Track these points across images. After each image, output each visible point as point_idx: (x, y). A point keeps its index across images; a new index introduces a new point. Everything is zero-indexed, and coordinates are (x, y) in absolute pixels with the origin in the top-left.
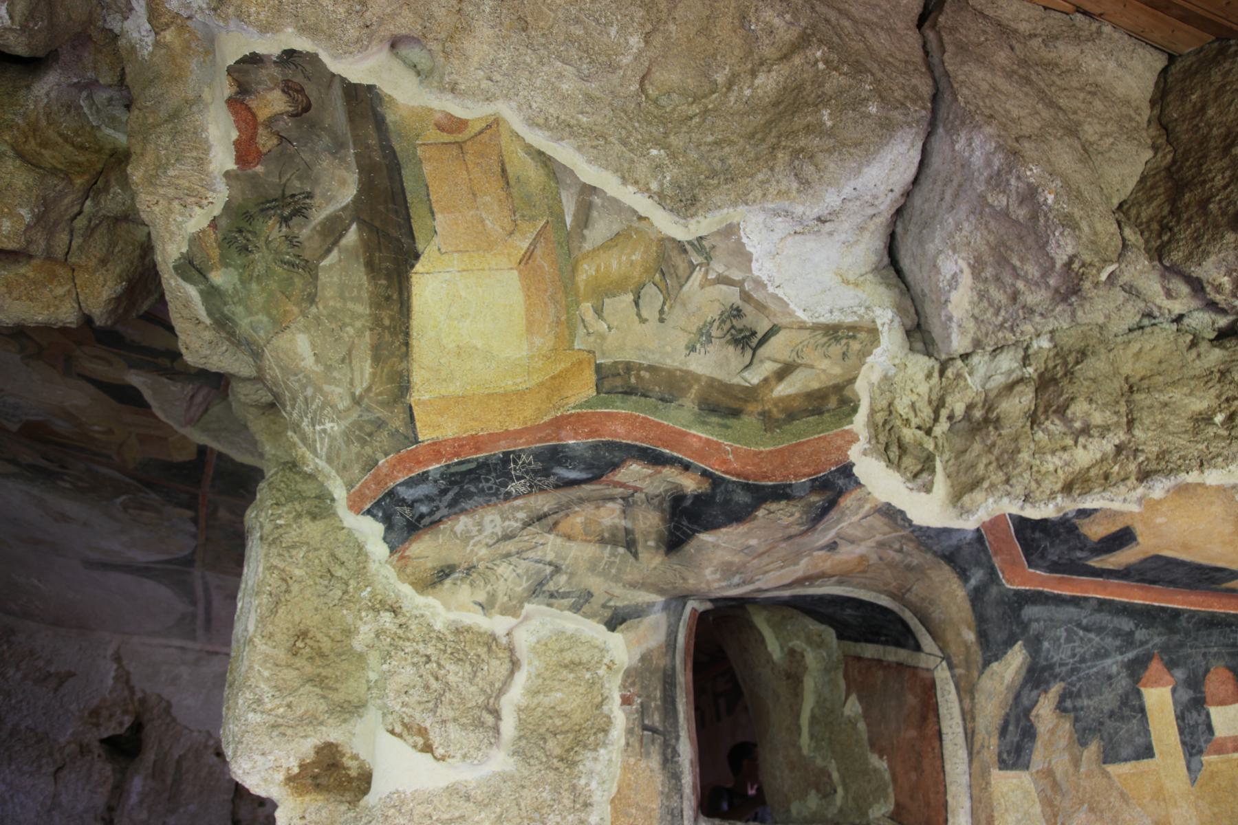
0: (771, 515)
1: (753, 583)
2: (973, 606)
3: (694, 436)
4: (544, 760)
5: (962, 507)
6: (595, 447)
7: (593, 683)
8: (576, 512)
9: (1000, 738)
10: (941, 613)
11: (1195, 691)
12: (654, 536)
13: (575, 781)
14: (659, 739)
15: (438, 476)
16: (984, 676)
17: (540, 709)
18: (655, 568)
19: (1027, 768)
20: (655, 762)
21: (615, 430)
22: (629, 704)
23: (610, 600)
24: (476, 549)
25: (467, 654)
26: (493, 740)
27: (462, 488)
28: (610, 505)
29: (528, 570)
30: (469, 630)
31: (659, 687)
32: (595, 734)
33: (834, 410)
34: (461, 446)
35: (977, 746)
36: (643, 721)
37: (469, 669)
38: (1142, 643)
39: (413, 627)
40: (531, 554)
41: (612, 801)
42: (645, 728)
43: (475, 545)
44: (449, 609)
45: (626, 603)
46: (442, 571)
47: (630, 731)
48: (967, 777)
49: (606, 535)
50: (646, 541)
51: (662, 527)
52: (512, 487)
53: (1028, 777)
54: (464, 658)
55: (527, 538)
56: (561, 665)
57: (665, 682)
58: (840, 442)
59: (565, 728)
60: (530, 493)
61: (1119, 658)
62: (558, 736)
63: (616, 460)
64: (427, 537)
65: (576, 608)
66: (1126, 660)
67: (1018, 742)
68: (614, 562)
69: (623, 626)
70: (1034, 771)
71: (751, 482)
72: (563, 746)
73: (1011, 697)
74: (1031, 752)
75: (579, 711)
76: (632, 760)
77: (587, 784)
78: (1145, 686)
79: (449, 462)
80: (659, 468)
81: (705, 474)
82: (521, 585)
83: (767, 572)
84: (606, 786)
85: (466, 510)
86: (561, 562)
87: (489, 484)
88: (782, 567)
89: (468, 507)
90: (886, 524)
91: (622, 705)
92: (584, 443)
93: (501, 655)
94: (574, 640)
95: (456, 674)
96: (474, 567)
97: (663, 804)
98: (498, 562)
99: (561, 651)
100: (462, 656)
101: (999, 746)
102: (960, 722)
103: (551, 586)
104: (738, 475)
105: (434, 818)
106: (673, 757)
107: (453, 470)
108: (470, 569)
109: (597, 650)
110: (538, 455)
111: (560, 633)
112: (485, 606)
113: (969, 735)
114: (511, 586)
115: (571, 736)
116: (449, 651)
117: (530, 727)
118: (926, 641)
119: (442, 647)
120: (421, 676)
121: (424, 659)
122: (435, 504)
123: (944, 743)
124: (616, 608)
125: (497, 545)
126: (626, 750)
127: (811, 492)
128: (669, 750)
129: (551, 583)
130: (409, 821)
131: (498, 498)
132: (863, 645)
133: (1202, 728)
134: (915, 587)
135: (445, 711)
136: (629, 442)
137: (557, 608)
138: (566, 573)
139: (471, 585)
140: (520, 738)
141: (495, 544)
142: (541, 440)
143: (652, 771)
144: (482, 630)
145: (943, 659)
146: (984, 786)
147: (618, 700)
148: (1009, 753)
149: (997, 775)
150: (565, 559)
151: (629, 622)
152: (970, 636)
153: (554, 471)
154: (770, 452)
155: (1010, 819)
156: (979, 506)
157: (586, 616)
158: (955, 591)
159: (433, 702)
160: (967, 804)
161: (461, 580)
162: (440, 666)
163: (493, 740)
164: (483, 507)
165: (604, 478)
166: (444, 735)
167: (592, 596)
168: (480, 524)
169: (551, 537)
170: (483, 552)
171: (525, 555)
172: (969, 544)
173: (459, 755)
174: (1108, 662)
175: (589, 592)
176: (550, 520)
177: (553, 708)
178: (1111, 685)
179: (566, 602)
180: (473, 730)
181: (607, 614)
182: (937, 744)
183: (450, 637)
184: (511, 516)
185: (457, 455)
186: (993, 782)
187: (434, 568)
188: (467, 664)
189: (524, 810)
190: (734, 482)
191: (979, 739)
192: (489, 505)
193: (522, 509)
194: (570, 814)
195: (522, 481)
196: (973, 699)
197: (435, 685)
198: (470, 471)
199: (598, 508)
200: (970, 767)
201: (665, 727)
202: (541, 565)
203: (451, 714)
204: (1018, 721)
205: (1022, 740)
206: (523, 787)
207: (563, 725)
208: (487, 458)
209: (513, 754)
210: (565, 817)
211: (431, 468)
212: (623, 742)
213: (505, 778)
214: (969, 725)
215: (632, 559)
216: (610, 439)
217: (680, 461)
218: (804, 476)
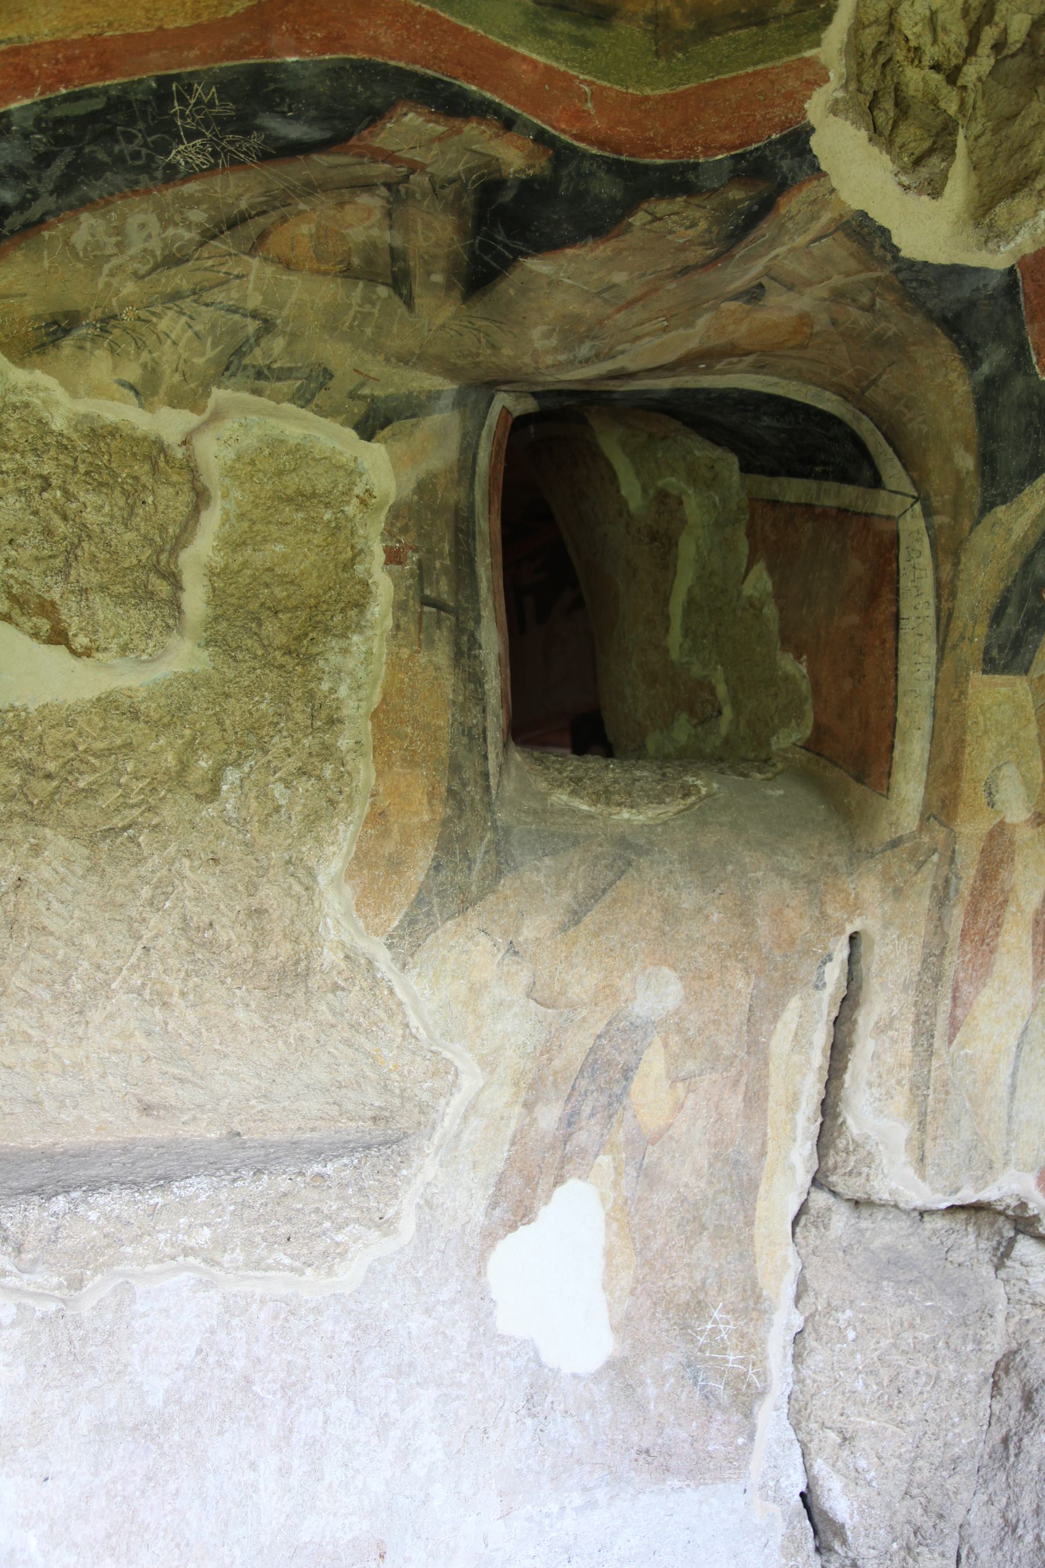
0: (657, 224)
1: (614, 357)
2: (979, 410)
3: (524, 58)
4: (260, 652)
5: (991, 226)
6: (337, 71)
7: (338, 528)
8: (300, 213)
9: (991, 626)
10: (924, 422)
12: (442, 264)
13: (313, 685)
14: (449, 620)
15: (29, 124)
16: (979, 527)
17: (248, 572)
18: (443, 326)
19: (1026, 672)
20: (442, 655)
21: (375, 38)
22: (399, 563)
23: (363, 385)
24: (115, 282)
25: (115, 475)
26: (171, 622)
27: (79, 152)
28: (364, 199)
29: (213, 326)
30: (114, 431)
31: (448, 536)
32: (343, 610)
33: (787, 16)
34: (70, 60)
35: (954, 636)
36: (422, 590)
37: (122, 502)
39: (11, 425)
40: (219, 296)
41: (374, 715)
42: (426, 601)
43: (112, 274)
44: (74, 394)
45: (391, 390)
46: (55, 323)
47: (400, 607)
48: (932, 683)
49: (356, 261)
50: (429, 273)
51: (457, 246)
52: (182, 154)
53: (1026, 685)
54: (111, 482)
55: (210, 263)
56: (280, 498)
57: (457, 530)
58: (792, 83)
59: (292, 602)
60: (213, 168)
62: (280, 616)
63: (378, 102)
64: (19, 256)
65: (303, 399)
67: (1018, 634)
68: (370, 314)
69: (387, 431)
70: (1036, 676)
71: (624, 158)
72: (290, 630)
73: (1018, 561)
74: (1036, 647)
75: (315, 574)
76: (405, 653)
77: (333, 690)
79: (48, 95)
80: (457, 123)
81: (542, 138)
82: (203, 354)
83: (638, 338)
84: (363, 693)
85: (91, 201)
86: (273, 312)
87: (134, 146)
88: (665, 330)
89: (94, 195)
90: (852, 254)
91: (386, 564)
92: (316, 63)
93: (175, 478)
94: (301, 455)
95: (99, 509)
96: (115, 317)
97: (455, 720)
98: (158, 309)
99: (280, 473)
100: (106, 477)
101: (988, 637)
102: (932, 601)
103: (257, 357)
104: (601, 144)
105: (81, 748)
106: (470, 649)
107: (59, 112)
108: (107, 321)
109: (341, 473)
110: (226, 85)
111: (275, 444)
112: (139, 388)
113: (943, 621)
114: (185, 355)
115: (303, 615)
116: (82, 468)
117: (234, 601)
118: (893, 472)
119: (70, 462)
120: (36, 513)
121: (38, 482)
122: (29, 185)
123: (901, 632)
124: (373, 398)
125: (154, 276)
126: (394, 637)
127: (730, 180)
128: (465, 638)
129: (257, 352)
130: (39, 754)
131: (153, 178)
132: (784, 480)
134: (884, 377)
135: (84, 574)
136: (402, 64)
137: (270, 398)
138: (284, 333)
139: (112, 351)
140: (216, 619)
141: (149, 273)
142: (230, 53)
143: (437, 669)
144: (138, 433)
145: (917, 499)
146: (955, 697)
147: (380, 556)
148: (1001, 649)
149: (977, 679)
150: (281, 307)
151: (396, 425)
152: (967, 462)
153: (258, 121)
154: (664, 98)
155: (988, 745)
156: (1021, 225)
157: (320, 412)
158: (951, 384)
159: (62, 557)
160: (927, 723)
161: (93, 340)
162: (67, 494)
163: (171, 622)
164: (124, 197)
165: (353, 141)
166: (87, 613)
167: (331, 377)
168: (119, 231)
169: (255, 262)
170: (129, 288)
171: (207, 297)
172: (991, 297)
173: (114, 646)
175: (325, 370)
176: (252, 229)
177: (270, 570)
179: (285, 386)
180: (136, 605)
181: (359, 409)
182: (890, 635)
183: (82, 444)
184: (177, 218)
185: (64, 79)
186: (970, 691)
187: (38, 317)
188: (117, 493)
189: (230, 731)
190: (594, 157)
191: (958, 625)
192: (135, 193)
193: (198, 203)
194: (306, 736)
195: (198, 142)
196: (956, 564)
197: (62, 528)
198: (93, 117)
199: (341, 205)
201: (457, 601)
202: (237, 317)
203: (95, 578)
204: (1023, 599)
205: (1025, 629)
206: (227, 696)
207: (289, 597)
208: (125, 88)
209: (207, 645)
210: (298, 741)
211: (13, 106)
212: (389, 623)
213: (194, 682)
214: (945, 605)
215: (402, 309)
216: (366, 56)
217: (495, 110)
218: (722, 148)
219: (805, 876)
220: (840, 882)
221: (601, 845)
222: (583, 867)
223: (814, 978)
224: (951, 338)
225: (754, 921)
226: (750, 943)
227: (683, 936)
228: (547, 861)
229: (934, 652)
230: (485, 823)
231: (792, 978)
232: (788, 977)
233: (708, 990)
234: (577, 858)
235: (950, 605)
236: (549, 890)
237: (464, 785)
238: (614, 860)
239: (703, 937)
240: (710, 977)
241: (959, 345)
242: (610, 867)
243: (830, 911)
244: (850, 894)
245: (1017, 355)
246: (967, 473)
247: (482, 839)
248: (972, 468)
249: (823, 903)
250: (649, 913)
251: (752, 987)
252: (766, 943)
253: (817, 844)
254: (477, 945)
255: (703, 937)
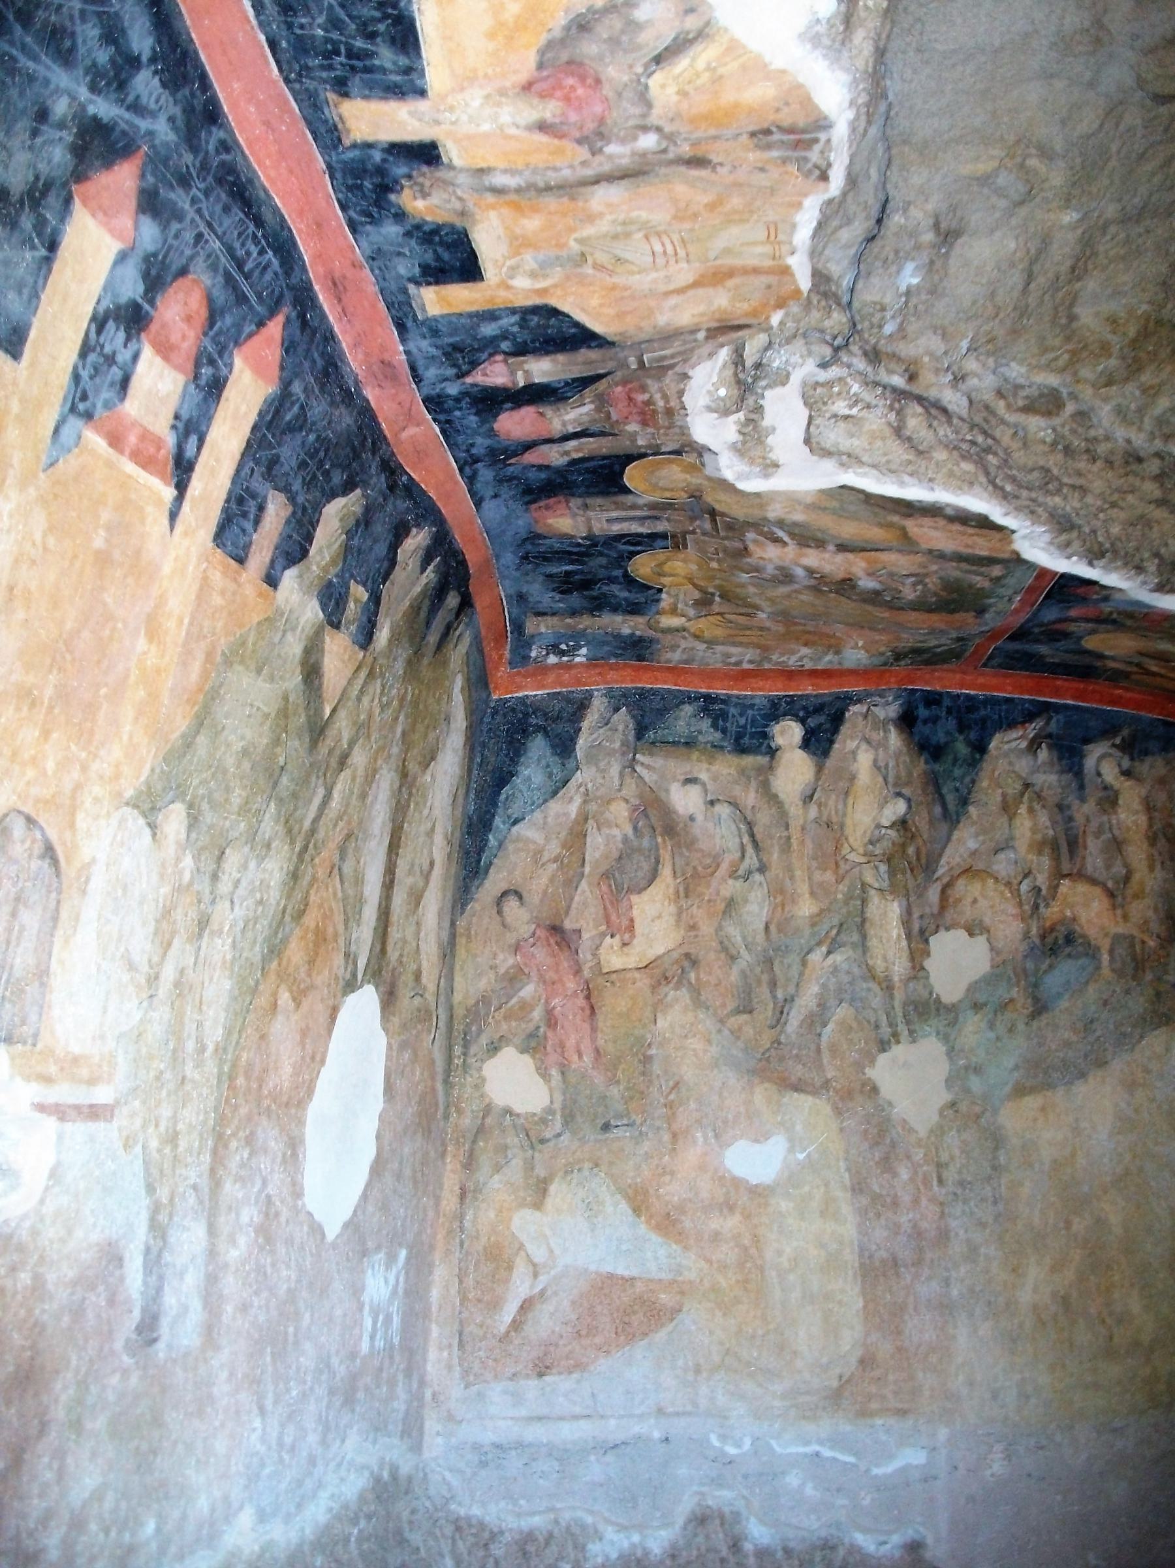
11: (146, 292)
38: (136, 107)
61: (83, 93)
66: (91, 110)
78: (85, 203)
133: (116, 373)
174: (61, 78)
178: (35, 133)
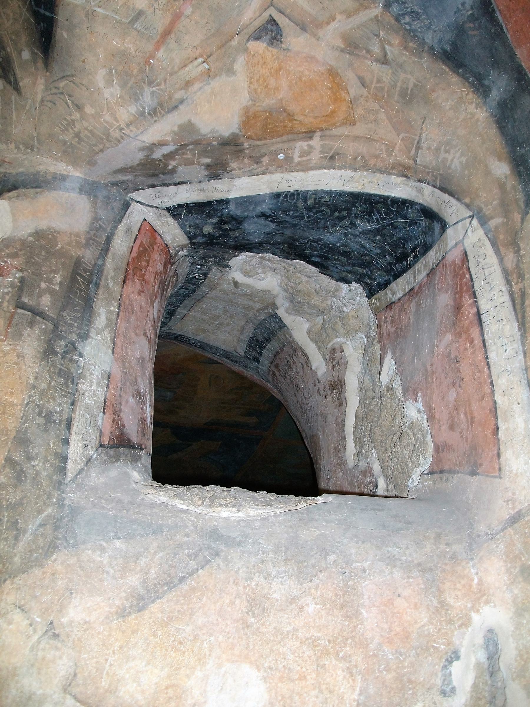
12: (24, 38)
36: (20, 297)
45: (21, 170)
48: (521, 357)
50: (20, 53)
69: (13, 193)
102: (504, 289)
113: (518, 301)
151: (21, 191)
182: (475, 332)
196: (517, 251)
200: (523, 344)
219: (419, 564)
220: (459, 568)
221: (187, 535)
222: (161, 554)
223: (439, 682)
224: (458, 74)
225: (358, 613)
226: (353, 638)
227: (270, 628)
228: (118, 543)
229: (516, 329)
230: (49, 497)
231: (410, 681)
232: (405, 679)
233: (300, 695)
234: (155, 544)
235: (521, 285)
236: (112, 571)
237: (29, 458)
238: (201, 550)
239: (296, 630)
240: (302, 678)
241: (467, 79)
242: (194, 556)
243: (450, 600)
244: (472, 580)
245: (518, 80)
246: (506, 177)
247: (39, 512)
248: (508, 172)
249: (441, 592)
250: (232, 603)
251: (357, 691)
252: (373, 639)
253: (433, 535)
254: (10, 623)
255: (296, 630)
